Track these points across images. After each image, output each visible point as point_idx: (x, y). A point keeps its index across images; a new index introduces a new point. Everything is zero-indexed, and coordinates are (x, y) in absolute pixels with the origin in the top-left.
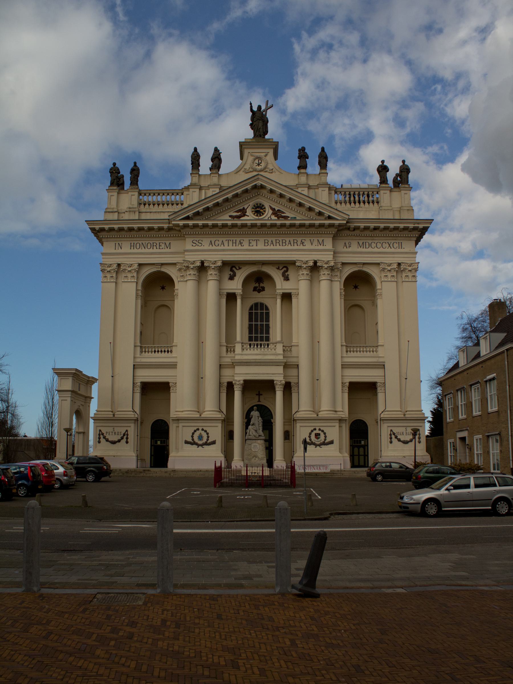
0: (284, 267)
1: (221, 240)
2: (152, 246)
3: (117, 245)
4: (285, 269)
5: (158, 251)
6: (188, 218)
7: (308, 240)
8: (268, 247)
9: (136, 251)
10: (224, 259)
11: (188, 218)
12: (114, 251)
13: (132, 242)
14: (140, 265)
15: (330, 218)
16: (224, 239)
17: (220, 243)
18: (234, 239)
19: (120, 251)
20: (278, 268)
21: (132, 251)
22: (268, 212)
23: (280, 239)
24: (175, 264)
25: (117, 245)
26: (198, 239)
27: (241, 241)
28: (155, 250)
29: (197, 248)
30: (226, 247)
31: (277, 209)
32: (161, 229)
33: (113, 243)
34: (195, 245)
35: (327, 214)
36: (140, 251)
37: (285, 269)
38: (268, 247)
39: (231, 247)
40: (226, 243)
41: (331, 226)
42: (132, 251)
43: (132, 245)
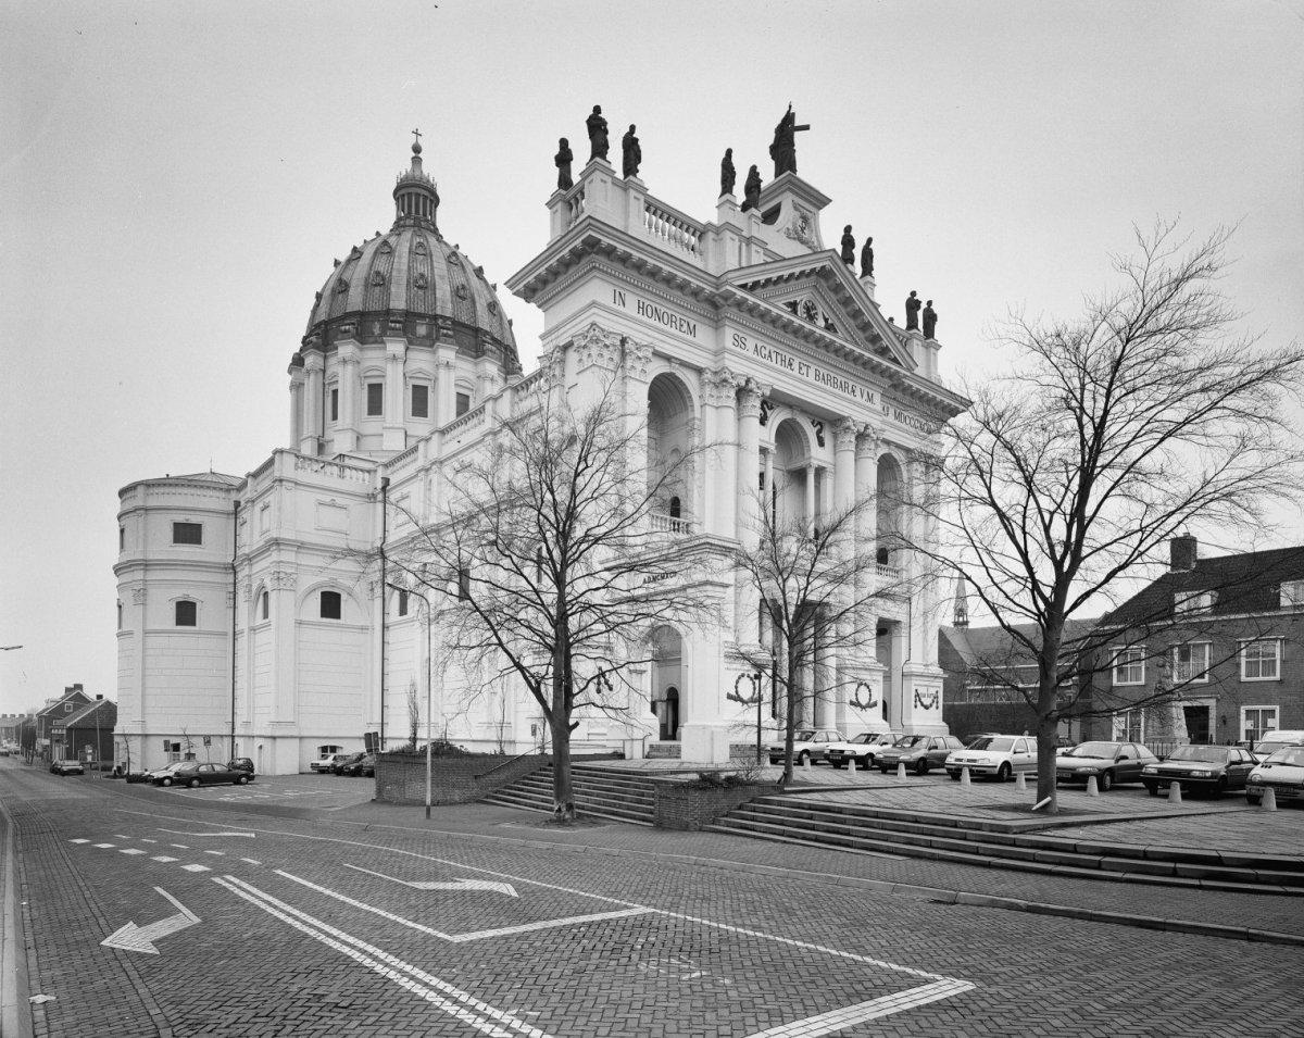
0: (820, 423)
1: (768, 347)
2: (671, 321)
4: (819, 427)
5: (677, 332)
6: (743, 286)
7: (859, 387)
9: (645, 318)
10: (775, 387)
11: (743, 286)
12: (612, 305)
13: (642, 300)
15: (895, 361)
16: (773, 349)
17: (767, 353)
18: (784, 354)
20: (813, 423)
21: (640, 316)
22: (821, 323)
23: (832, 375)
24: (699, 371)
25: (617, 294)
26: (741, 335)
28: (673, 330)
29: (738, 349)
31: (830, 322)
32: (696, 293)
33: (612, 288)
35: (894, 353)
36: (651, 321)
37: (819, 427)
40: (774, 356)
41: (892, 376)
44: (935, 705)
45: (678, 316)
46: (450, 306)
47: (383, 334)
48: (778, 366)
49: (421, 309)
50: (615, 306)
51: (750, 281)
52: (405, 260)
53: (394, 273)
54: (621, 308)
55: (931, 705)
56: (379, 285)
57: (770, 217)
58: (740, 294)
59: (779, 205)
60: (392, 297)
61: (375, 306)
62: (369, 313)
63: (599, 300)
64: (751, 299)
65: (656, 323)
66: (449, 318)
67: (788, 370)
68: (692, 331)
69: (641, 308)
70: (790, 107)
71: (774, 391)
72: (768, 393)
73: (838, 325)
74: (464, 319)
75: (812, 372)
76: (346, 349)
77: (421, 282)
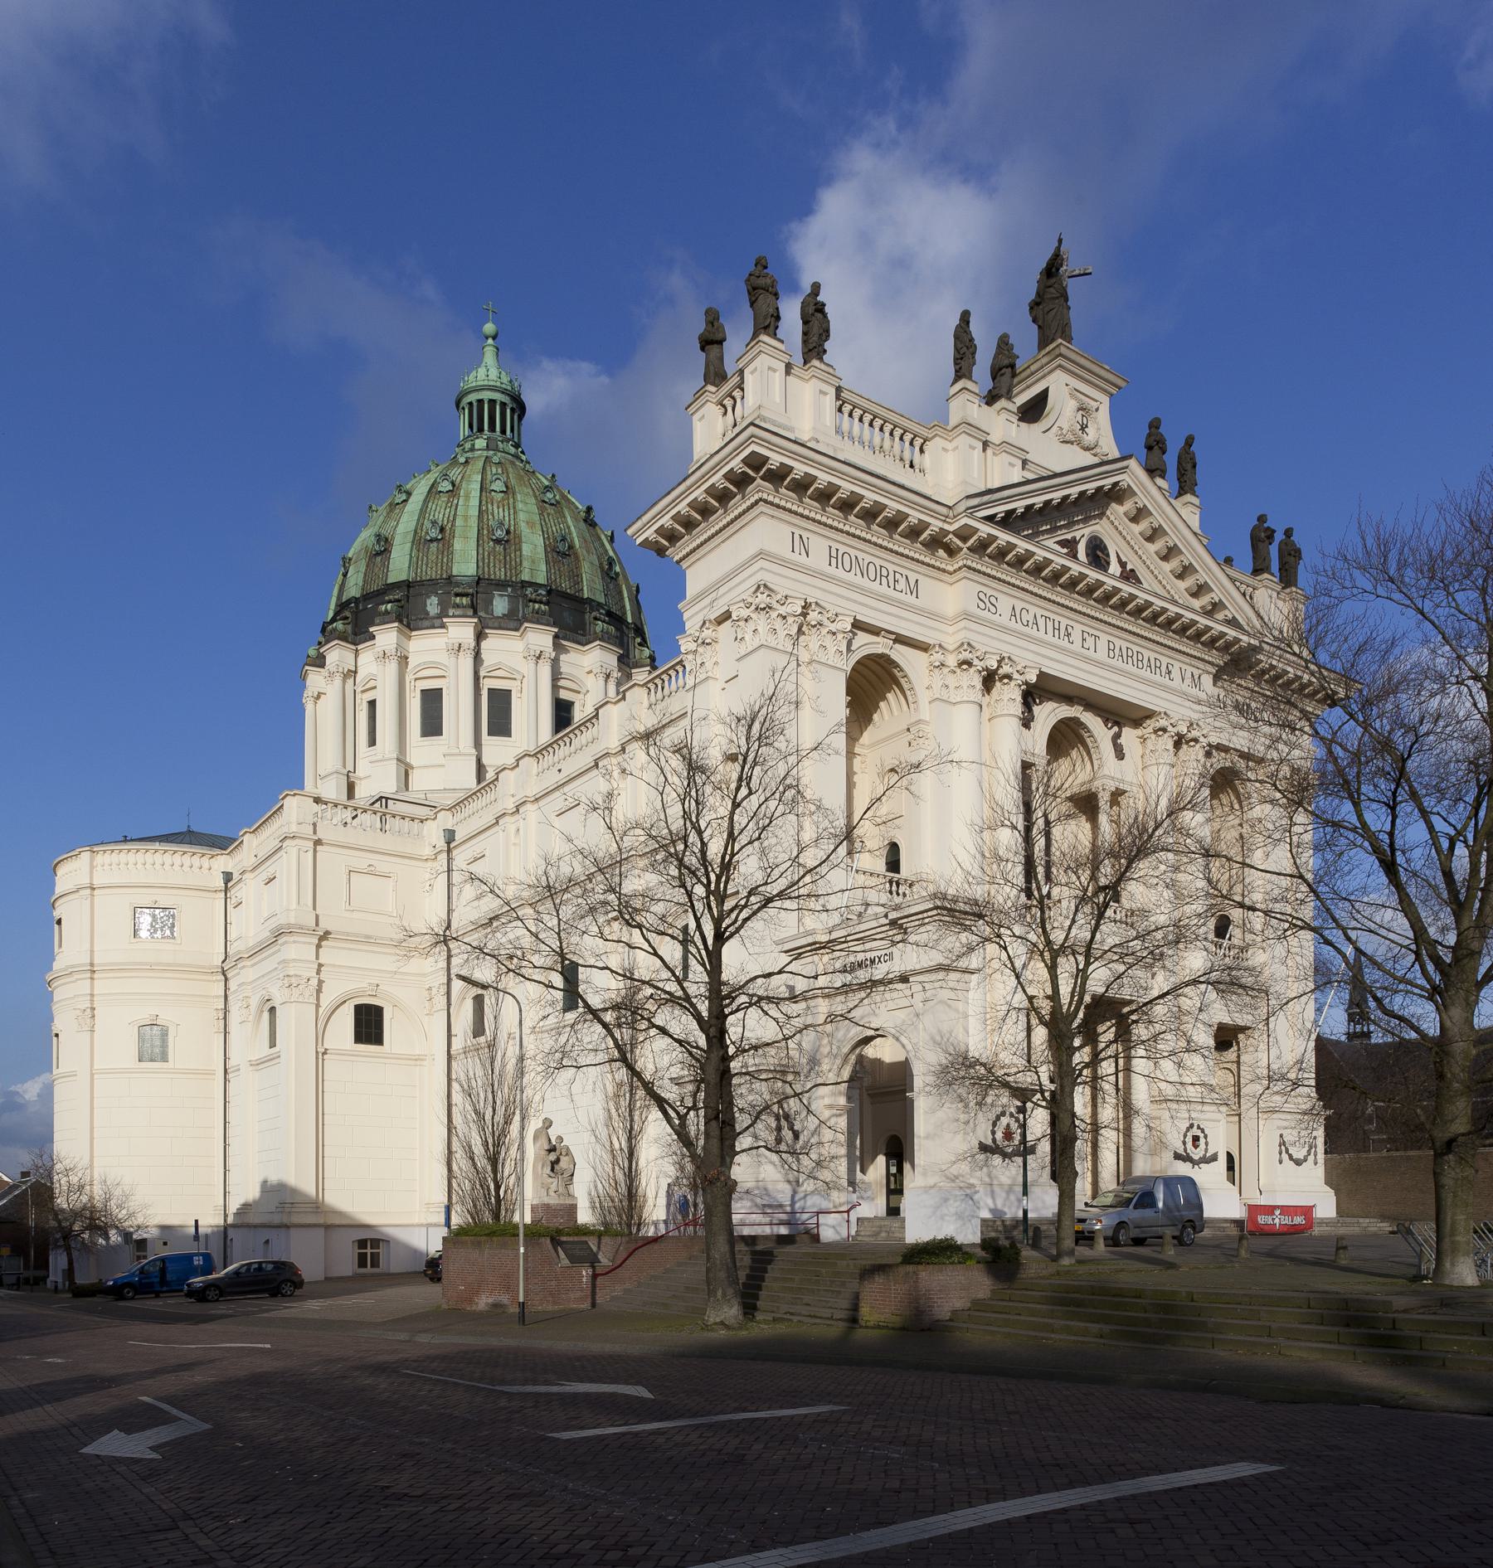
1: (1033, 610)
2: (879, 576)
3: (797, 537)
5: (891, 592)
8: (1113, 662)
9: (840, 573)
12: (788, 555)
13: (835, 545)
14: (858, 625)
16: (1039, 612)
18: (1057, 618)
19: (803, 559)
21: (832, 570)
22: (1114, 568)
24: (923, 647)
25: (797, 537)
26: (989, 592)
27: (1070, 629)
28: (884, 589)
29: (985, 614)
30: (1041, 635)
34: (982, 605)
36: (850, 577)
38: (1113, 662)
39: (1049, 638)
40: (1041, 622)
42: (832, 570)
43: (834, 554)
44: (1311, 1158)
45: (891, 568)
46: (543, 567)
47: (443, 614)
48: (1049, 638)
49: (501, 574)
50: (795, 557)
51: (1000, 510)
52: (475, 502)
53: (459, 522)
54: (803, 559)
55: (1305, 1160)
56: (436, 540)
57: (1033, 411)
58: (985, 530)
59: (1046, 391)
60: (457, 557)
61: (431, 573)
62: (421, 583)
63: (767, 548)
64: (1004, 537)
65: (859, 580)
66: (541, 586)
67: (1065, 643)
68: (914, 589)
69: (834, 558)
70: (1060, 241)
71: (1042, 675)
72: (1033, 678)
73: (1142, 573)
74: (565, 586)
75: (1102, 644)
76: (386, 636)
77: (499, 534)
